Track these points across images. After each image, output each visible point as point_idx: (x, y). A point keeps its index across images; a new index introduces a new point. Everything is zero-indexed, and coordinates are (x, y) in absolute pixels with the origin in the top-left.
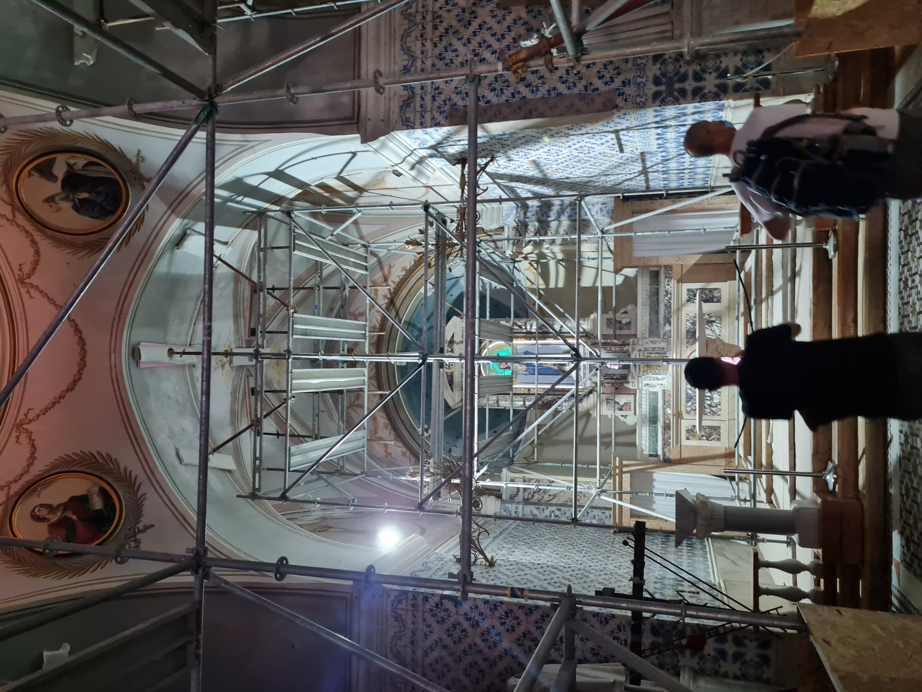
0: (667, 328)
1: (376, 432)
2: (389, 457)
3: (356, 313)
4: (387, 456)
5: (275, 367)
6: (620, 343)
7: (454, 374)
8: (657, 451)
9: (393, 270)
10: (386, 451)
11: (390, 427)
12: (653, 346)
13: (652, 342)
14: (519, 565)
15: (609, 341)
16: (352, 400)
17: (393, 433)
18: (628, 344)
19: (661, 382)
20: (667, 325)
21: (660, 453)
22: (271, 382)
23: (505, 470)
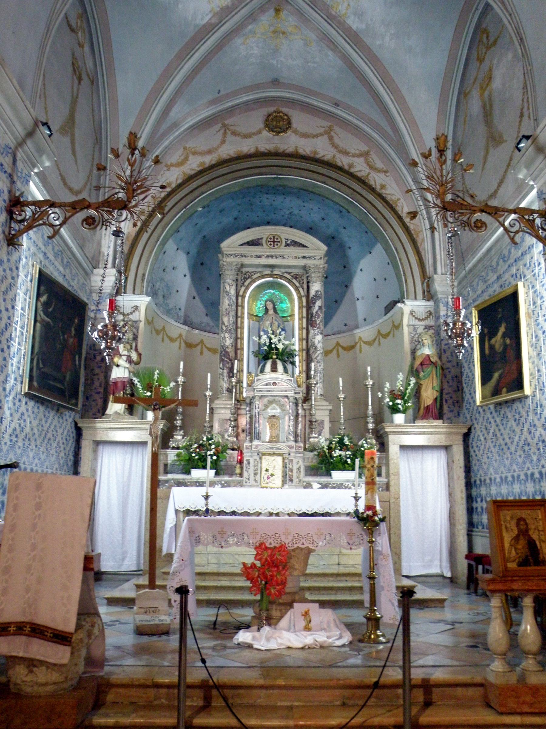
0: (316, 485)
1: (194, 153)
2: (165, 168)
3: (332, 133)
4: (166, 166)
5: (272, 29)
6: (299, 431)
7: (260, 247)
8: (171, 473)
9: (382, 175)
10: (172, 165)
11: (201, 168)
12: (295, 470)
13: (299, 469)
14: (10, 280)
15: (300, 419)
16: (231, 128)
17: (193, 172)
18: (296, 441)
19: (252, 478)
20: (320, 486)
21: (170, 476)
22: (255, 20)
23: (148, 299)
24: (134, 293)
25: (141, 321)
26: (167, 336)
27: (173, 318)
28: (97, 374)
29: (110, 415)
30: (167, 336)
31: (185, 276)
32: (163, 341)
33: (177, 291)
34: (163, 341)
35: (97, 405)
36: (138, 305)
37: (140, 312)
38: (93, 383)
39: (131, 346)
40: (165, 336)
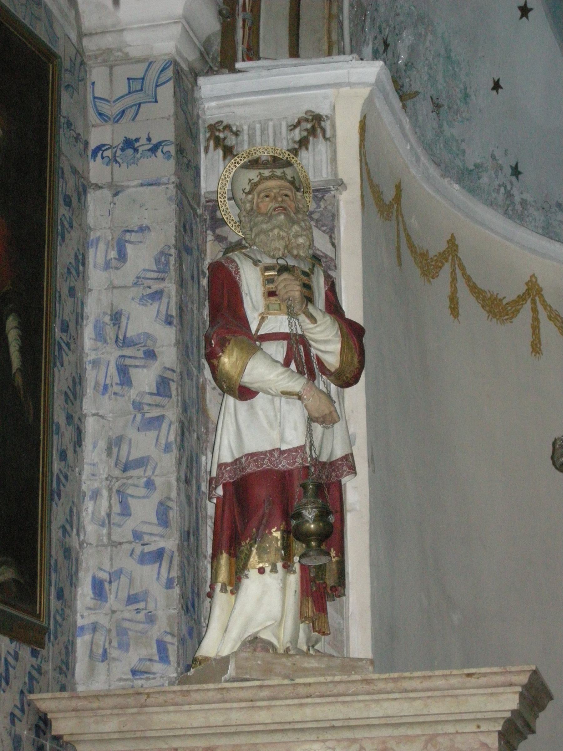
24: (294, 52)
25: (341, 185)
26: (474, 289)
27: (492, 204)
28: (142, 462)
29: (224, 662)
30: (474, 289)
31: (525, 11)
32: (454, 309)
33: (497, 86)
34: (454, 309)
35: (151, 619)
36: (324, 111)
37: (330, 140)
38: (126, 512)
39: (307, 287)
40: (461, 284)
